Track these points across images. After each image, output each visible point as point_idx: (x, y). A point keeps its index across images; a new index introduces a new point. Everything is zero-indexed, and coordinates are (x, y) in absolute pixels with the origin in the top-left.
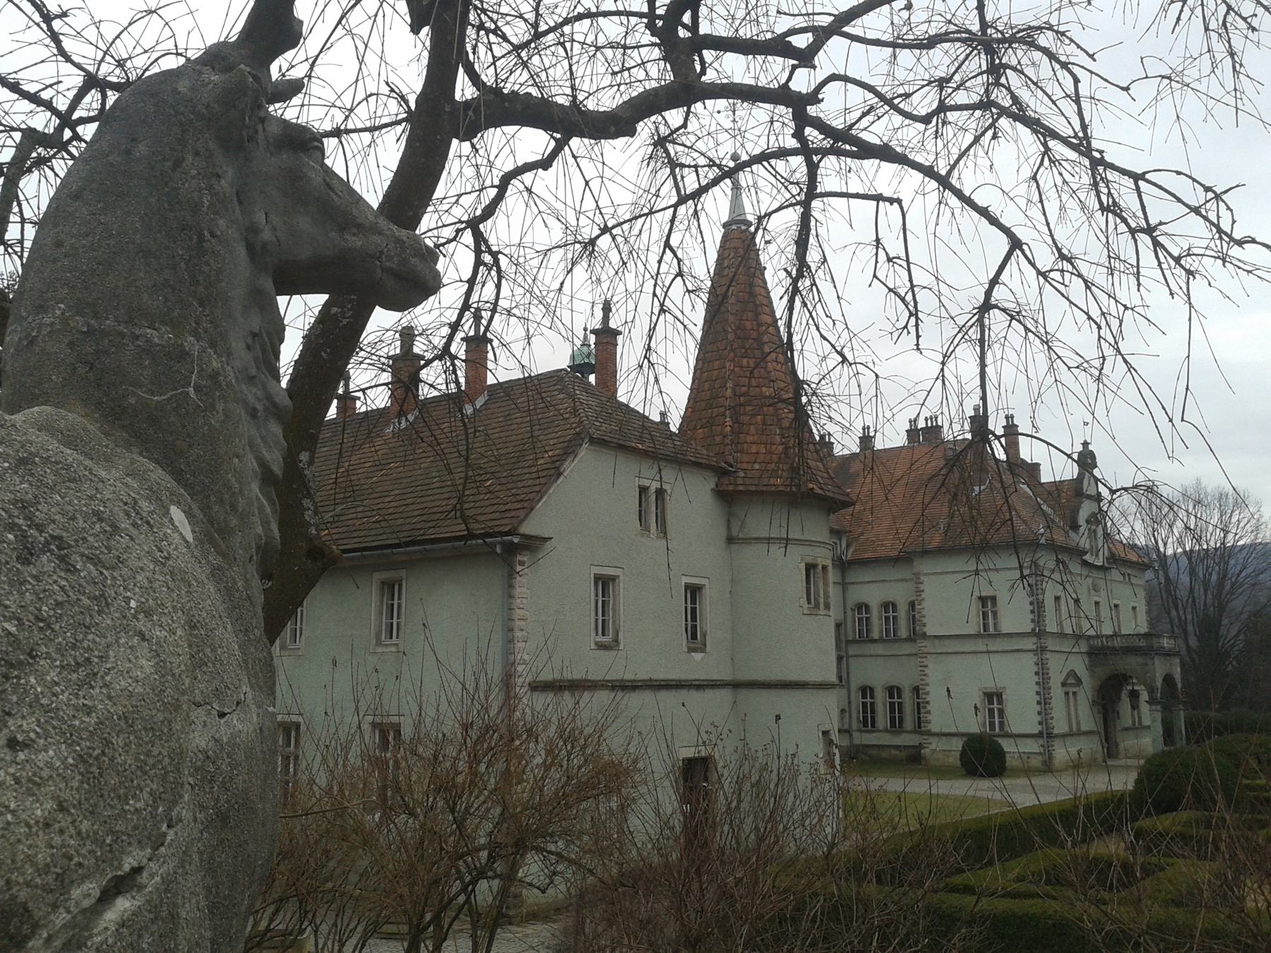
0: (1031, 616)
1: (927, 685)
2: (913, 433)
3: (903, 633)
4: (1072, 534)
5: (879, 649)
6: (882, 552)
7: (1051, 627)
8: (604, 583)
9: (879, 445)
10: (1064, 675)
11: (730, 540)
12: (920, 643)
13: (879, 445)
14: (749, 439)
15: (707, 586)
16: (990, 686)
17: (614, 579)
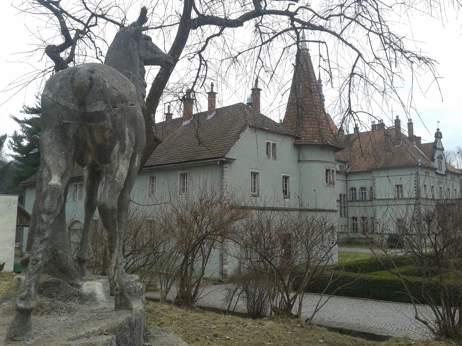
2: (374, 126)
3: (368, 198)
4: (432, 162)
6: (361, 169)
8: (254, 175)
11: (299, 161)
12: (374, 202)
14: (306, 126)
15: (291, 177)
17: (258, 173)
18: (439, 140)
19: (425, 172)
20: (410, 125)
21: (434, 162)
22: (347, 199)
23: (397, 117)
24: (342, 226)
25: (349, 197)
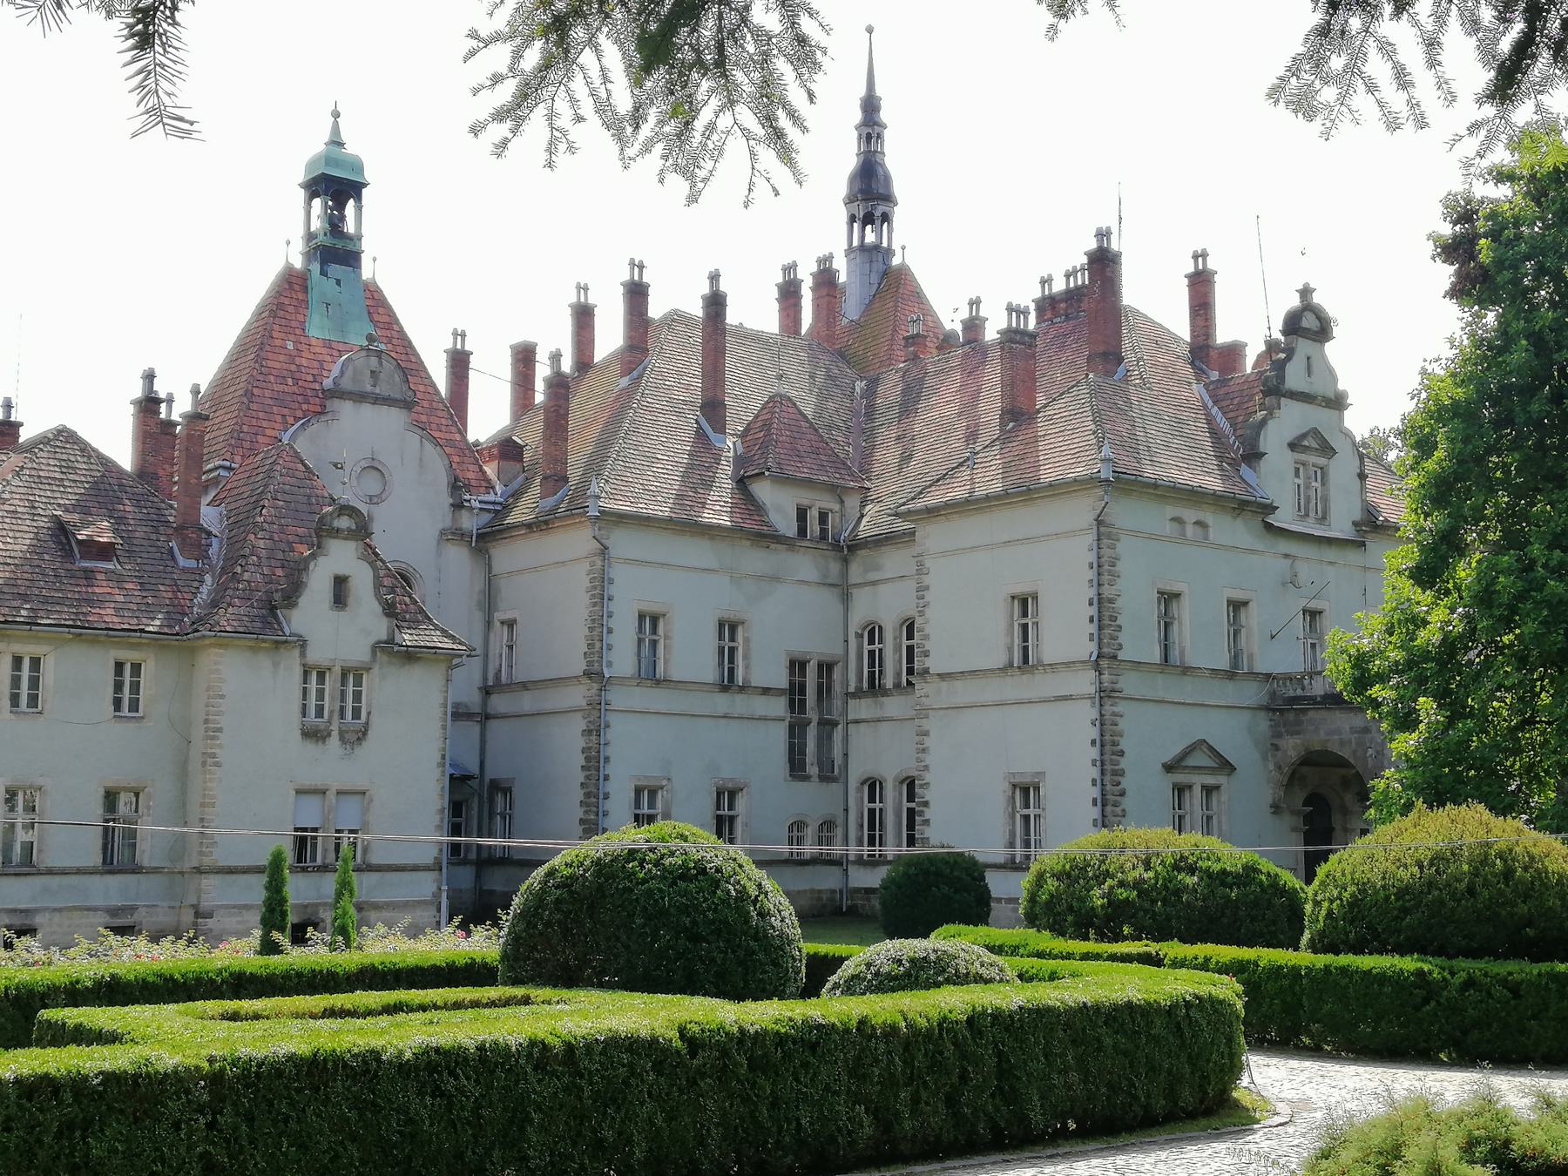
1: (926, 768)
4: (1244, 469)
5: (893, 705)
7: (1139, 643)
10: (1176, 750)
16: (1025, 767)
25: (850, 675)
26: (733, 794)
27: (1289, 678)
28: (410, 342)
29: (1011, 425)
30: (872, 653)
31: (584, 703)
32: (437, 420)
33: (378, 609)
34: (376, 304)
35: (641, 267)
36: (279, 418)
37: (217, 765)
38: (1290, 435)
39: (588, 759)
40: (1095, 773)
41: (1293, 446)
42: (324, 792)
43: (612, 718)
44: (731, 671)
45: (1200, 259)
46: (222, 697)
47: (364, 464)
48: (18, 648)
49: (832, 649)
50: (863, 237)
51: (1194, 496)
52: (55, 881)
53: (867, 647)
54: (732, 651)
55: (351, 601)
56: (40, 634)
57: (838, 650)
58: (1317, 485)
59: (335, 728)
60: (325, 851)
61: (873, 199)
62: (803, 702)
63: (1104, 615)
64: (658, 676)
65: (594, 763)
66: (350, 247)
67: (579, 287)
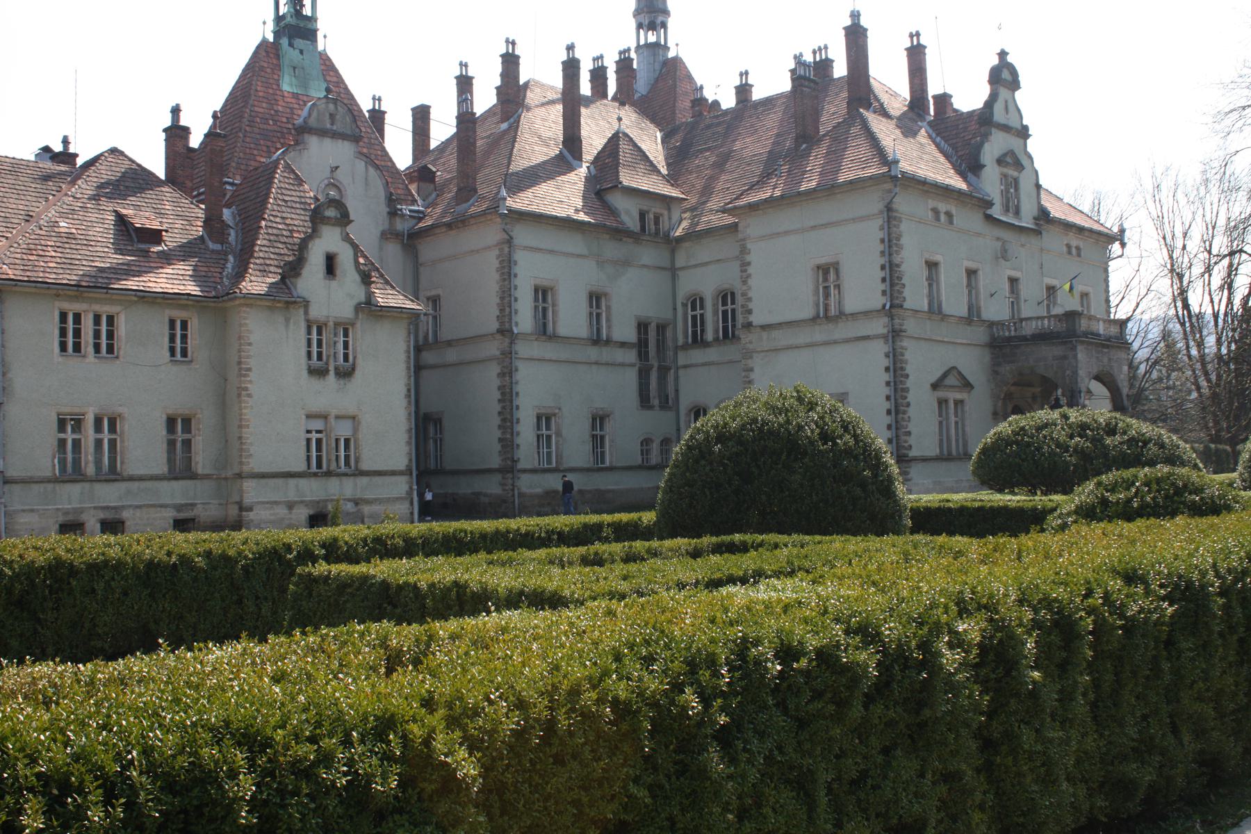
0: (882, 287)
5: (712, 354)
9: (757, 95)
10: (938, 374)
13: (757, 95)
18: (1004, 93)
19: (936, 212)
20: (916, 55)
21: (978, 177)
22: (675, 339)
23: (855, 15)
24: (646, 442)
25: (681, 333)
26: (602, 419)
27: (1000, 324)
28: (353, 96)
29: (804, 146)
30: (694, 317)
31: (498, 353)
32: (375, 152)
33: (357, 278)
34: (328, 67)
35: (513, 43)
36: (265, 149)
37: (249, 396)
38: (997, 153)
39: (503, 394)
40: (887, 391)
41: (1000, 161)
42: (325, 417)
43: (520, 365)
44: (598, 330)
45: (915, 38)
46: (250, 344)
47: (326, 182)
48: (97, 308)
49: (667, 315)
50: (646, 39)
51: (946, 191)
52: (136, 484)
53: (690, 313)
54: (598, 315)
55: (338, 272)
56: (114, 297)
57: (669, 315)
58: (1012, 190)
59: (331, 368)
60: (329, 461)
61: (654, 12)
62: (647, 353)
63: (892, 276)
64: (548, 333)
65: (507, 396)
66: (309, 26)
67: (461, 64)
